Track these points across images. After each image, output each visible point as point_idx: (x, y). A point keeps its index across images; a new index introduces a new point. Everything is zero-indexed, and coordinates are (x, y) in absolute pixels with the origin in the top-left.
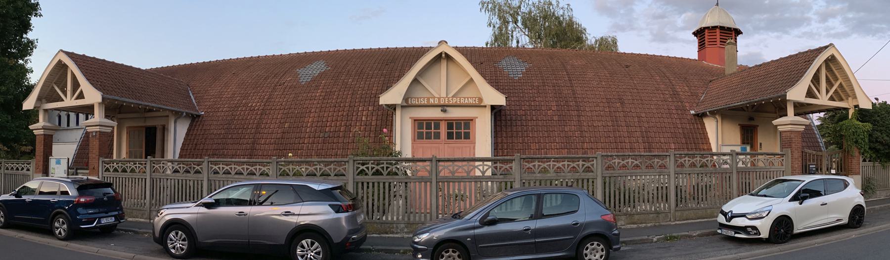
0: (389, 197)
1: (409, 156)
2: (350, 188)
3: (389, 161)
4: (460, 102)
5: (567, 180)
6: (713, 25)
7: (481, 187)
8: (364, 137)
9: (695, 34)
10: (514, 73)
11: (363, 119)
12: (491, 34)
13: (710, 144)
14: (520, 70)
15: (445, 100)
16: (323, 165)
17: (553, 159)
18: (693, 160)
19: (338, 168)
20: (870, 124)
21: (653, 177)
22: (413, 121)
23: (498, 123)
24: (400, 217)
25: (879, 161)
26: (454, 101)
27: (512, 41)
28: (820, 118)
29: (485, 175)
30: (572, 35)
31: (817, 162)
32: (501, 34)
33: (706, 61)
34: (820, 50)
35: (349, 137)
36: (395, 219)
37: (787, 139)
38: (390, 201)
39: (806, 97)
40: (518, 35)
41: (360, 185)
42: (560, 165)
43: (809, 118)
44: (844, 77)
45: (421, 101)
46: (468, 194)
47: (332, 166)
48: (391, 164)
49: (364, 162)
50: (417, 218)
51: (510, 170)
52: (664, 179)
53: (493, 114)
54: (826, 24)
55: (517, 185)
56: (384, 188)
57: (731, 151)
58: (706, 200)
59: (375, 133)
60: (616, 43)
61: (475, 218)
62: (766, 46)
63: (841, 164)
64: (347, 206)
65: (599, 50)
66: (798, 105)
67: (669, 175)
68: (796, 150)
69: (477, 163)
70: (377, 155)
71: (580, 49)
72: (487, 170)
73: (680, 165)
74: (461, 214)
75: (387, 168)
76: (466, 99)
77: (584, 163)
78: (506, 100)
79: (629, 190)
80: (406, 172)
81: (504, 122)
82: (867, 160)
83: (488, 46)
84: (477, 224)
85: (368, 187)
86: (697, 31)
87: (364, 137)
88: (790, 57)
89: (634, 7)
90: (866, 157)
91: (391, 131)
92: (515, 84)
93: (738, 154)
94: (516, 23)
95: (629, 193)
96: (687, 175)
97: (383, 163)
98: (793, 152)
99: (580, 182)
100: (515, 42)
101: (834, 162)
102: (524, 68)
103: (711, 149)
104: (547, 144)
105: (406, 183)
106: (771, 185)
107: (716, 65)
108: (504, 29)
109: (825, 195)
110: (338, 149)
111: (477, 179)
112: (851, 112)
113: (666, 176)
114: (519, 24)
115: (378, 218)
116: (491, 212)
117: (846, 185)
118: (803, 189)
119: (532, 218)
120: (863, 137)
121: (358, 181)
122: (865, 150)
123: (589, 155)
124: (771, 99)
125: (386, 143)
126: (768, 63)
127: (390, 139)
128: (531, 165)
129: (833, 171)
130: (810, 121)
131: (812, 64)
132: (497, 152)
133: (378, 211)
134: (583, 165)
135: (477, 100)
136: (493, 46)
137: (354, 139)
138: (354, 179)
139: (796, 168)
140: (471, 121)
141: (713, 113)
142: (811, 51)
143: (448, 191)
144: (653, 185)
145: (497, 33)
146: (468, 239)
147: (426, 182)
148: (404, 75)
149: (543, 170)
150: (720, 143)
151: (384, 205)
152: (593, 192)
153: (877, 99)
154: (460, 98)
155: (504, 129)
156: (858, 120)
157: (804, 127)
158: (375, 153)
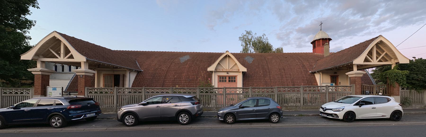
0: (210, 100)
1: (217, 87)
2: (198, 97)
13: (317, 83)
21: (295, 94)
23: (244, 77)
24: (214, 106)
33: (316, 53)
36: (212, 106)
38: (211, 101)
41: (201, 96)
42: (263, 90)
46: (235, 98)
48: (211, 89)
50: (219, 106)
52: (299, 95)
55: (250, 96)
56: (209, 97)
57: (326, 85)
58: (315, 103)
60: (282, 50)
61: (237, 106)
65: (277, 53)
69: (238, 89)
70: (207, 87)
72: (241, 91)
74: (233, 105)
75: (210, 91)
79: (286, 99)
80: (216, 92)
84: (238, 108)
85: (204, 97)
91: (211, 79)
93: (329, 86)
97: (208, 89)
99: (270, 95)
100: (250, 51)
103: (318, 85)
105: (216, 95)
111: (238, 94)
114: (251, 45)
119: (255, 106)
128: (254, 90)
133: (207, 104)
134: (271, 90)
140: (236, 77)
141: (319, 72)
143: (229, 97)
147: (222, 95)
151: (209, 102)
152: (274, 99)
155: (246, 79)
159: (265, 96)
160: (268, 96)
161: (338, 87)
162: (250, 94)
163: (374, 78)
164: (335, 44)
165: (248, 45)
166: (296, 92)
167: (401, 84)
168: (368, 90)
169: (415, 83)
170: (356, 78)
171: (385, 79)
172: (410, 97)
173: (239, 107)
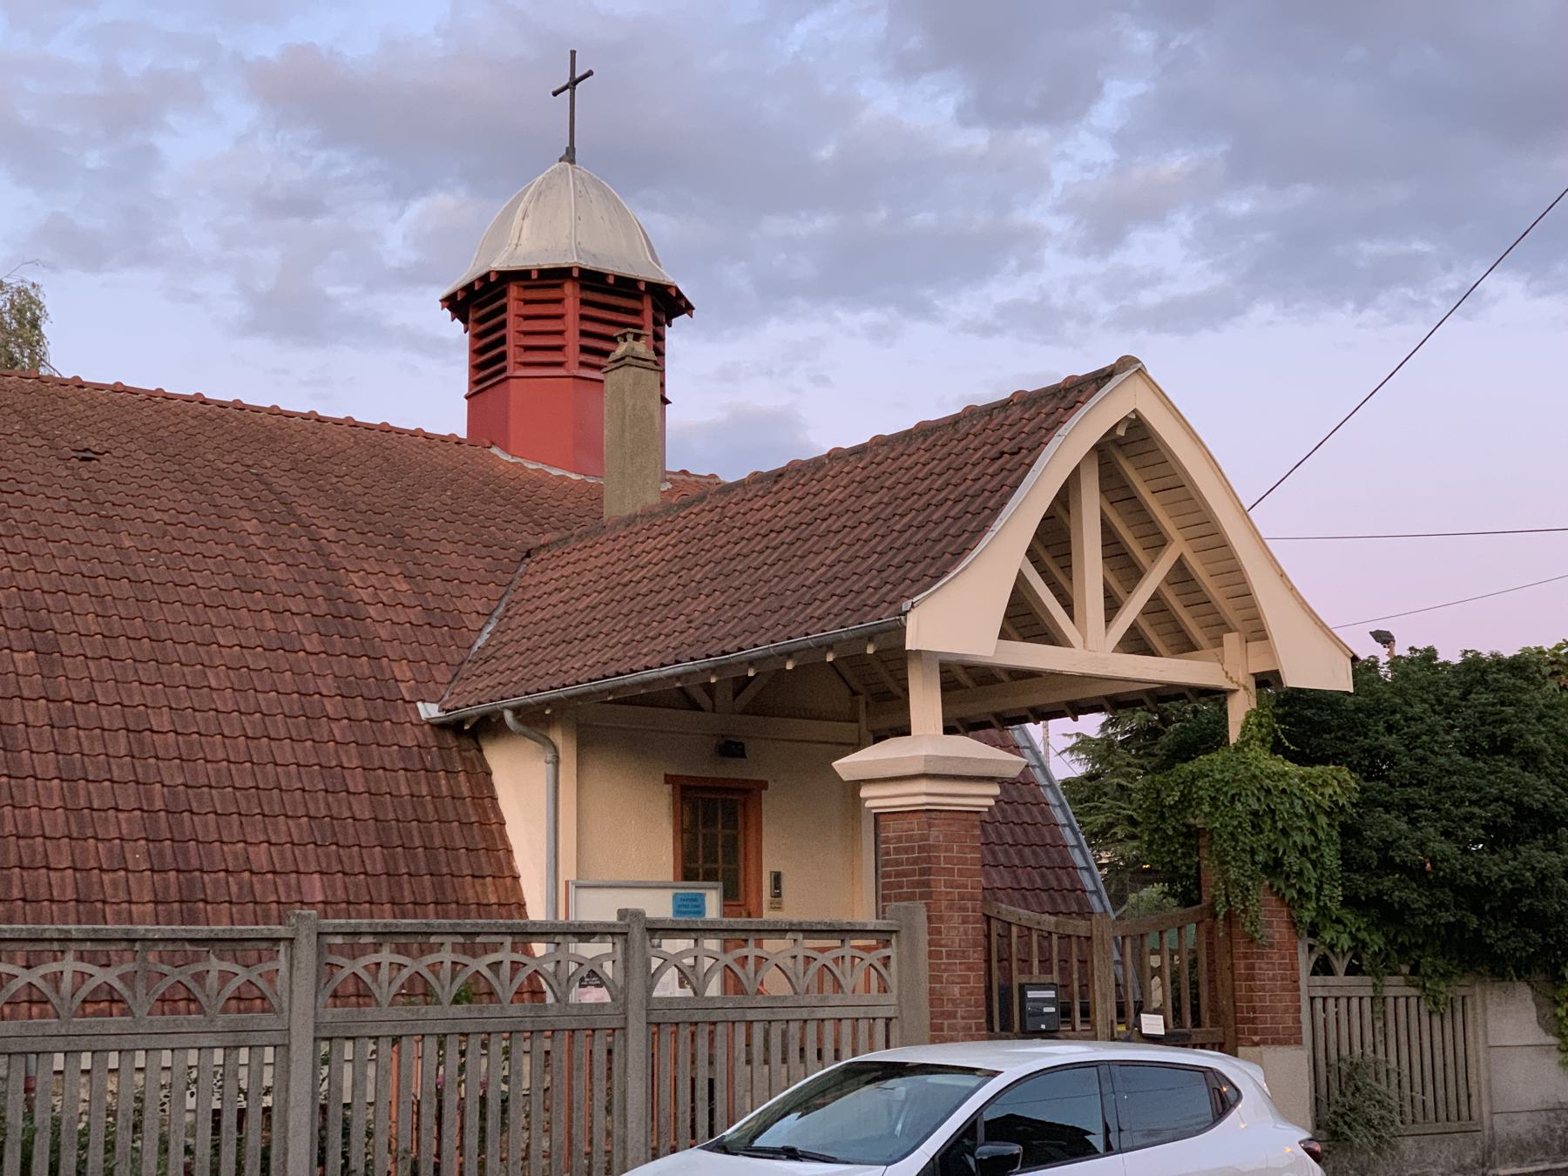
6: (548, 263)
9: (459, 304)
13: (516, 878)
18: (421, 965)
20: (1345, 773)
21: (192, 1057)
25: (1405, 969)
28: (1082, 745)
31: (1065, 971)
33: (505, 449)
34: (1072, 396)
37: (907, 850)
39: (1004, 635)
43: (1022, 742)
44: (1201, 530)
54: (1118, 258)
57: (623, 914)
60: (35, 324)
62: (821, 380)
63: (1195, 985)
66: (963, 678)
67: (287, 1047)
68: (950, 908)
73: (351, 989)
82: (1340, 965)
86: (468, 288)
88: (925, 430)
89: (160, 141)
90: (1331, 947)
93: (657, 930)
95: (55, 1149)
96: (385, 1045)
98: (941, 919)
101: (1158, 972)
103: (521, 906)
106: (823, 1093)
107: (556, 472)
109: (1109, 1150)
112: (1239, 710)
113: (269, 1051)
117: (1223, 1101)
118: (987, 1116)
120: (1309, 841)
122: (1323, 911)
124: (830, 647)
126: (817, 464)
129: (1153, 1024)
130: (1028, 759)
131: (1030, 465)
139: (953, 1001)
141: (535, 719)
142: (1024, 401)
144: (191, 1103)
150: (568, 871)
153: (1384, 638)
156: (1277, 748)
157: (995, 790)
161: (759, 945)
163: (1100, 836)
164: (728, 375)
166: (221, 1022)
167: (1307, 917)
168: (1046, 979)
169: (1405, 905)
170: (934, 832)
171: (1184, 855)
172: (1381, 1056)
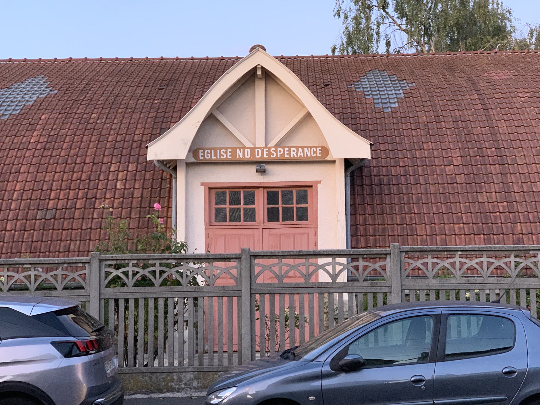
0: (166, 325)
1: (200, 249)
2: (93, 310)
3: (164, 261)
4: (289, 154)
5: (487, 291)
7: (331, 301)
8: (121, 218)
10: (384, 101)
11: (118, 186)
12: (342, 31)
14: (395, 96)
15: (263, 151)
16: (40, 270)
17: (460, 253)
19: (71, 276)
22: (207, 189)
23: (358, 190)
24: (186, 362)
26: (279, 154)
27: (378, 41)
29: (338, 280)
30: (485, 23)
32: (358, 30)
35: (93, 219)
36: (176, 363)
38: (166, 331)
40: (389, 31)
41: (112, 304)
42: (473, 263)
45: (221, 155)
46: (306, 315)
47: (59, 272)
48: (168, 265)
49: (119, 262)
50: (216, 362)
51: (382, 272)
53: (348, 174)
55: (395, 299)
56: (156, 308)
59: (140, 211)
64: (86, 343)
69: (321, 261)
70: (144, 251)
71: (502, 49)
72: (341, 271)
74: (297, 351)
75: (162, 272)
76: (300, 149)
77: (518, 260)
78: (372, 150)
80: (194, 279)
81: (367, 190)
83: (337, 53)
84: (327, 369)
85: (126, 308)
87: (121, 218)
91: (169, 207)
92: (387, 121)
94: (384, 8)
97: (154, 265)
99: (513, 294)
100: (383, 43)
102: (401, 91)
104: (446, 227)
105: (196, 299)
108: (364, 21)
110: (71, 240)
115: (145, 363)
116: (351, 347)
119: (424, 358)
121: (107, 297)
123: (527, 246)
125: (159, 229)
127: (166, 222)
128: (419, 264)
132: (357, 241)
133: (146, 351)
135: (319, 152)
136: (345, 53)
137: (101, 221)
138: (100, 294)
140: (309, 190)
143: (272, 310)
145: (351, 29)
146: (312, 398)
147: (230, 297)
148: (191, 107)
149: (440, 272)
151: (156, 338)
154: (290, 148)
155: (368, 200)
158: (139, 247)
159: (483, 298)
160: (503, 300)
162: (396, 286)
165: (370, 8)
173: (333, 364)
